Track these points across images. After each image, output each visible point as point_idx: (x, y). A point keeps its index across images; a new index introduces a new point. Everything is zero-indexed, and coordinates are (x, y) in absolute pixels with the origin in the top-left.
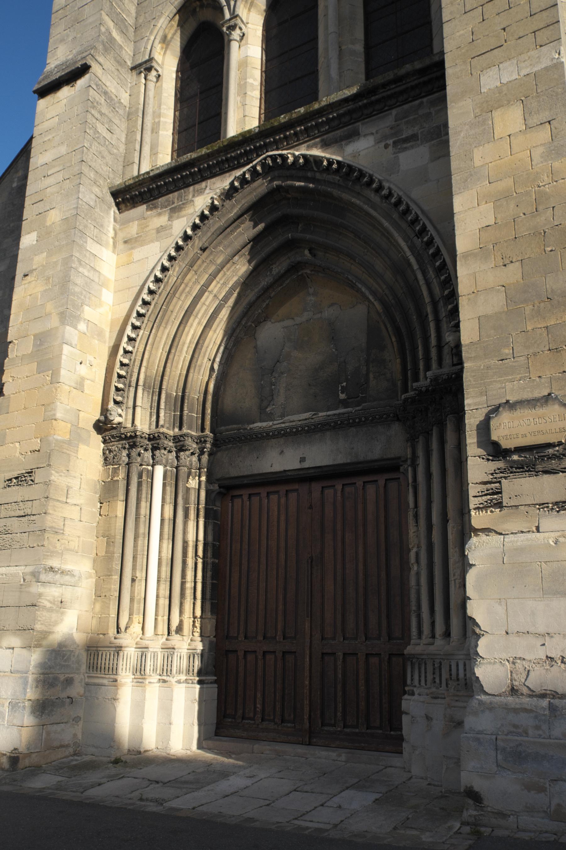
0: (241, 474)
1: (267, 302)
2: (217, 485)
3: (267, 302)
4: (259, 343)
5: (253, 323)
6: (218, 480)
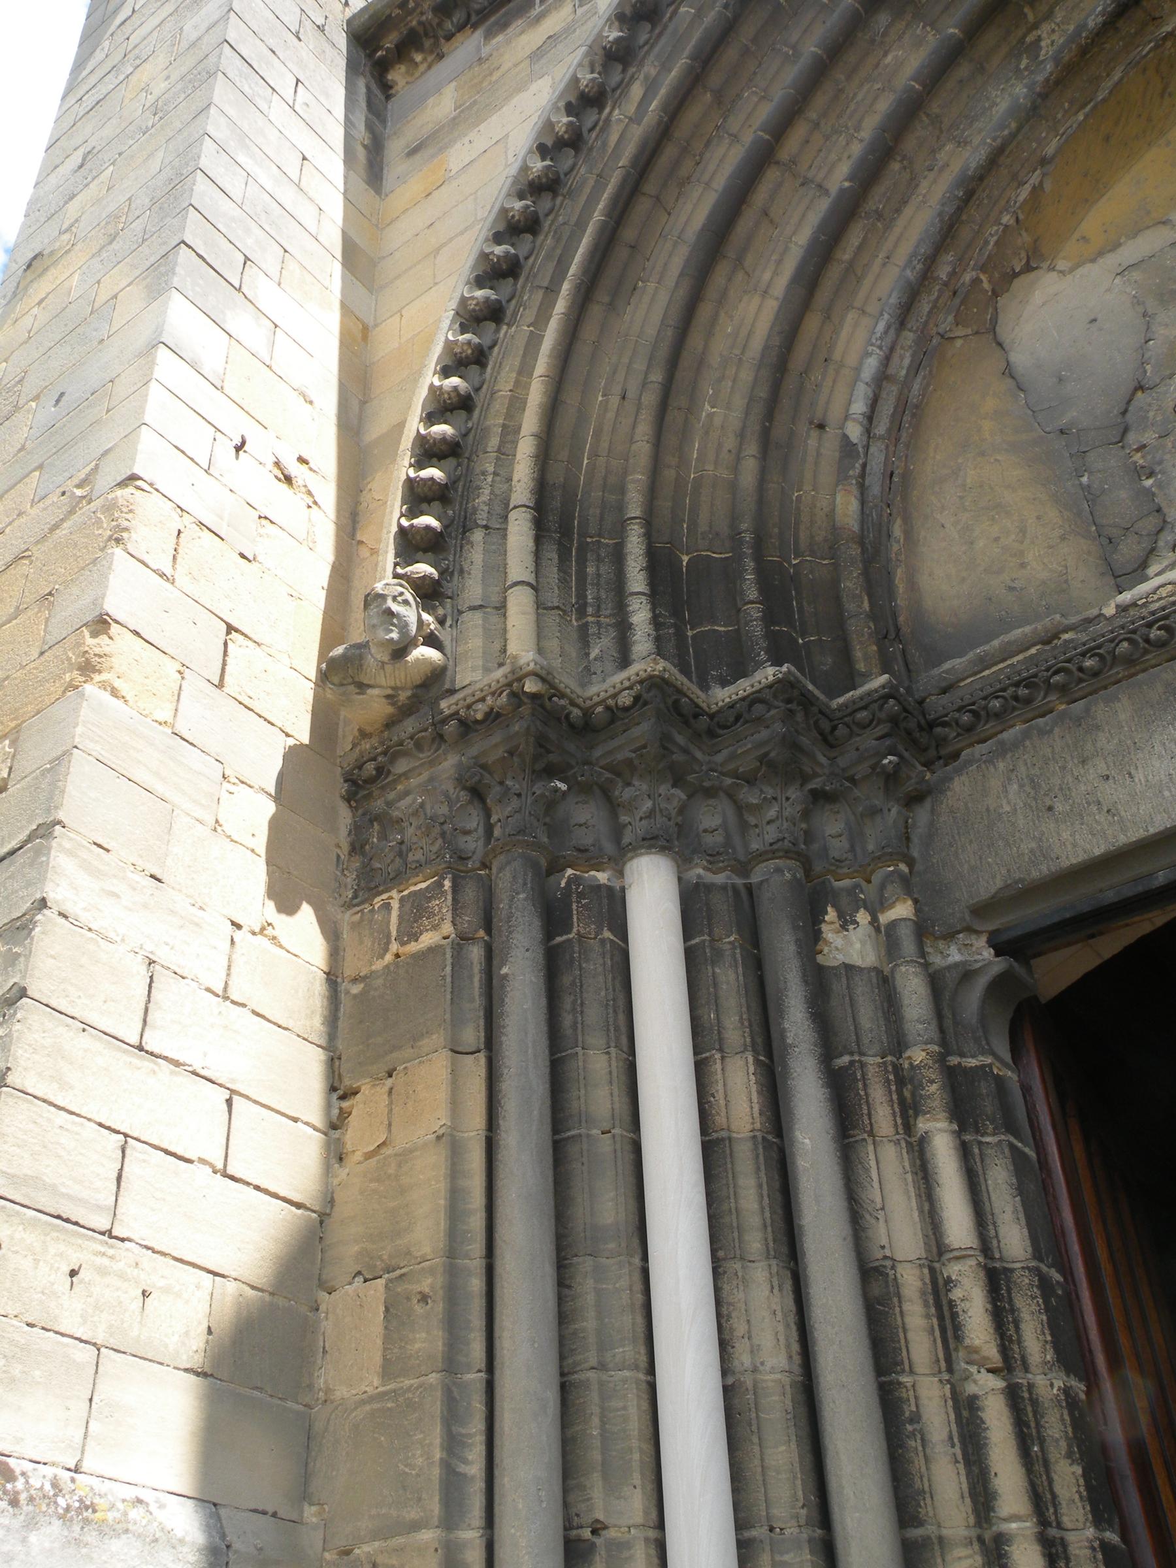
0: (1135, 834)
1: (1035, 178)
2: (981, 942)
3: (1035, 178)
4: (1020, 358)
5: (983, 268)
6: (981, 910)
